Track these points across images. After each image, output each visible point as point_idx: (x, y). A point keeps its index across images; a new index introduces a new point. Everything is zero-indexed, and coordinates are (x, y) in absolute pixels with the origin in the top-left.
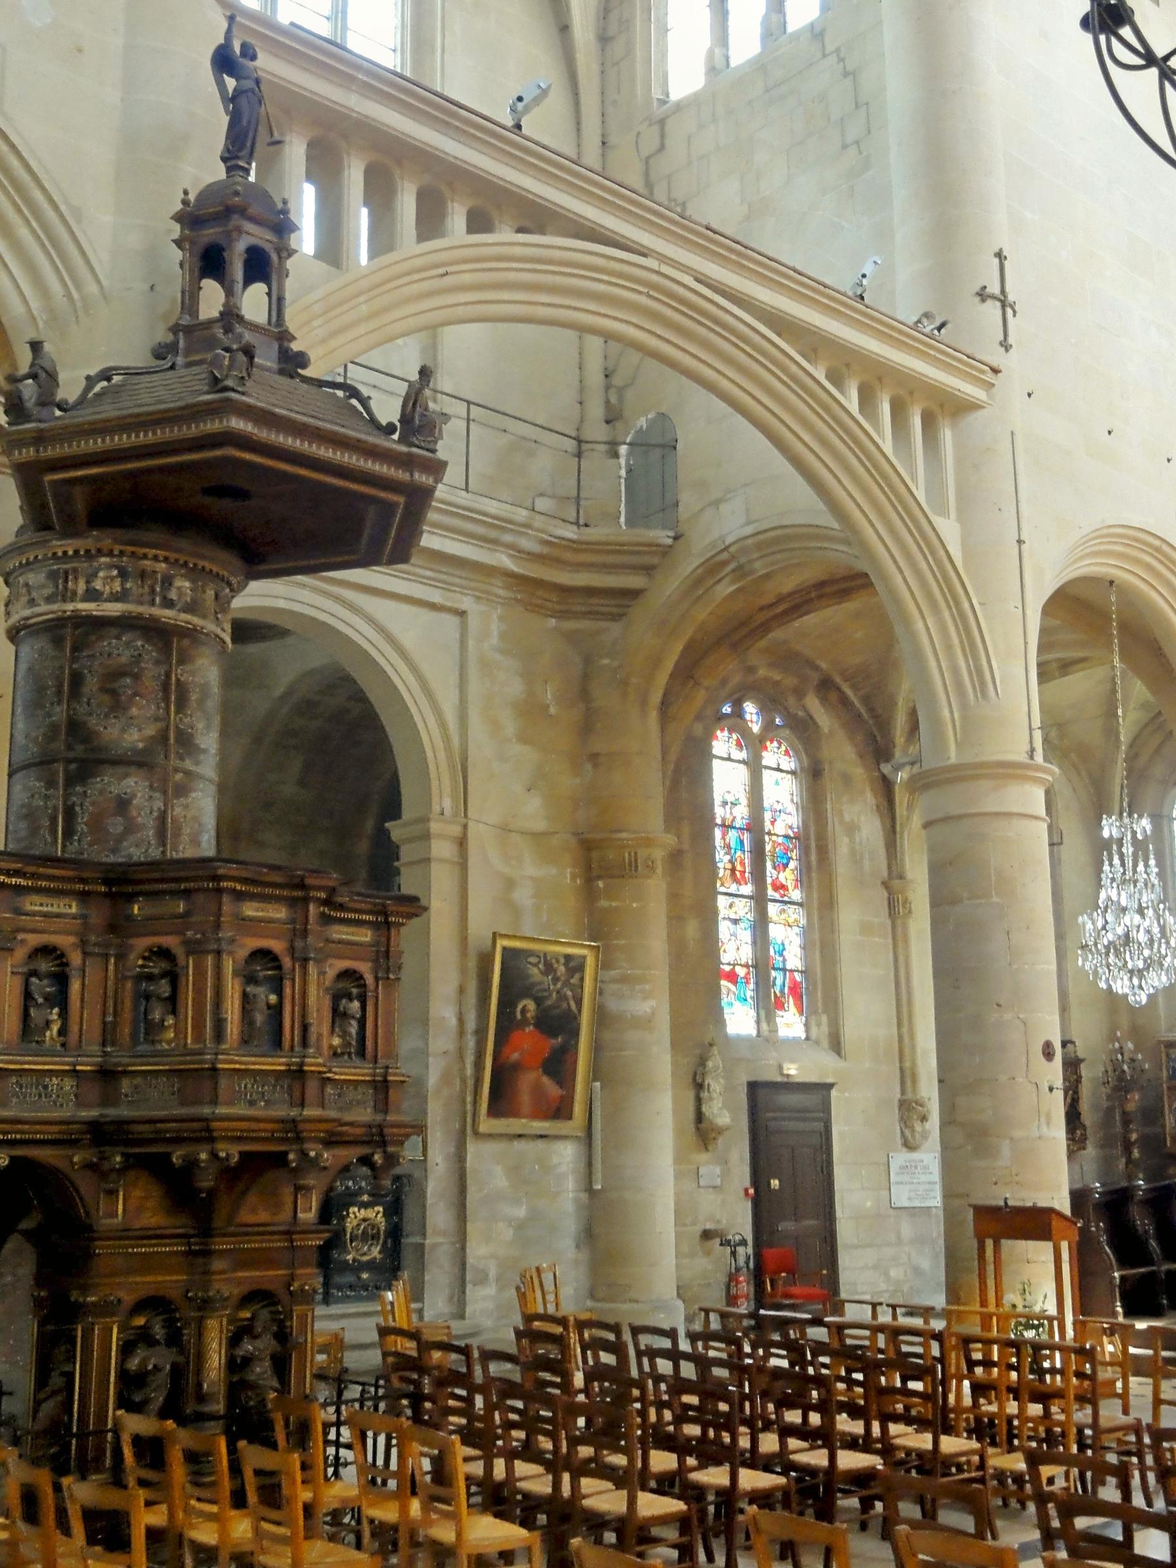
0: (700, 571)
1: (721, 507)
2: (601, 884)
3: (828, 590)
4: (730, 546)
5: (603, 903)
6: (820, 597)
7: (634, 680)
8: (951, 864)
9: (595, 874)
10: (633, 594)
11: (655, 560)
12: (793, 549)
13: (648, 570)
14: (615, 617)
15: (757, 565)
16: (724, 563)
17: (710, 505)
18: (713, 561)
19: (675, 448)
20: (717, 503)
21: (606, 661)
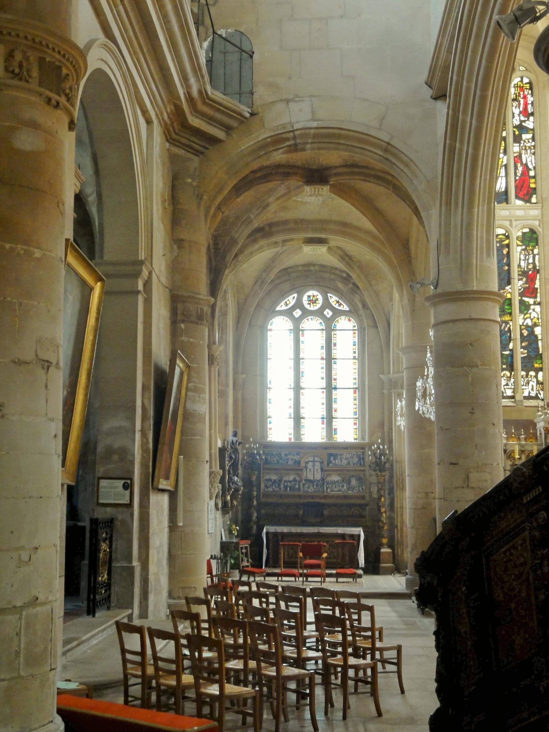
0: (269, 140)
1: (291, 104)
2: (183, 326)
3: (281, 170)
4: (297, 130)
5: (184, 338)
6: (276, 173)
7: (205, 197)
8: (471, 344)
9: (180, 317)
10: (214, 141)
11: (234, 124)
12: (338, 143)
13: (228, 129)
14: (197, 153)
15: (309, 146)
16: (288, 139)
17: (281, 100)
18: (280, 136)
19: (251, 57)
20: (288, 101)
21: (189, 180)
